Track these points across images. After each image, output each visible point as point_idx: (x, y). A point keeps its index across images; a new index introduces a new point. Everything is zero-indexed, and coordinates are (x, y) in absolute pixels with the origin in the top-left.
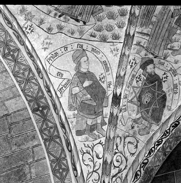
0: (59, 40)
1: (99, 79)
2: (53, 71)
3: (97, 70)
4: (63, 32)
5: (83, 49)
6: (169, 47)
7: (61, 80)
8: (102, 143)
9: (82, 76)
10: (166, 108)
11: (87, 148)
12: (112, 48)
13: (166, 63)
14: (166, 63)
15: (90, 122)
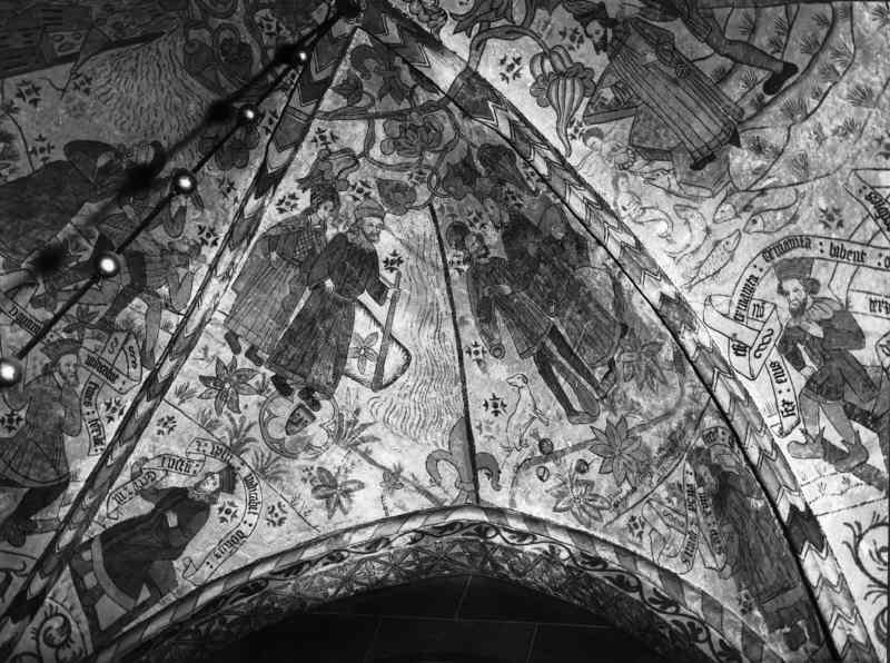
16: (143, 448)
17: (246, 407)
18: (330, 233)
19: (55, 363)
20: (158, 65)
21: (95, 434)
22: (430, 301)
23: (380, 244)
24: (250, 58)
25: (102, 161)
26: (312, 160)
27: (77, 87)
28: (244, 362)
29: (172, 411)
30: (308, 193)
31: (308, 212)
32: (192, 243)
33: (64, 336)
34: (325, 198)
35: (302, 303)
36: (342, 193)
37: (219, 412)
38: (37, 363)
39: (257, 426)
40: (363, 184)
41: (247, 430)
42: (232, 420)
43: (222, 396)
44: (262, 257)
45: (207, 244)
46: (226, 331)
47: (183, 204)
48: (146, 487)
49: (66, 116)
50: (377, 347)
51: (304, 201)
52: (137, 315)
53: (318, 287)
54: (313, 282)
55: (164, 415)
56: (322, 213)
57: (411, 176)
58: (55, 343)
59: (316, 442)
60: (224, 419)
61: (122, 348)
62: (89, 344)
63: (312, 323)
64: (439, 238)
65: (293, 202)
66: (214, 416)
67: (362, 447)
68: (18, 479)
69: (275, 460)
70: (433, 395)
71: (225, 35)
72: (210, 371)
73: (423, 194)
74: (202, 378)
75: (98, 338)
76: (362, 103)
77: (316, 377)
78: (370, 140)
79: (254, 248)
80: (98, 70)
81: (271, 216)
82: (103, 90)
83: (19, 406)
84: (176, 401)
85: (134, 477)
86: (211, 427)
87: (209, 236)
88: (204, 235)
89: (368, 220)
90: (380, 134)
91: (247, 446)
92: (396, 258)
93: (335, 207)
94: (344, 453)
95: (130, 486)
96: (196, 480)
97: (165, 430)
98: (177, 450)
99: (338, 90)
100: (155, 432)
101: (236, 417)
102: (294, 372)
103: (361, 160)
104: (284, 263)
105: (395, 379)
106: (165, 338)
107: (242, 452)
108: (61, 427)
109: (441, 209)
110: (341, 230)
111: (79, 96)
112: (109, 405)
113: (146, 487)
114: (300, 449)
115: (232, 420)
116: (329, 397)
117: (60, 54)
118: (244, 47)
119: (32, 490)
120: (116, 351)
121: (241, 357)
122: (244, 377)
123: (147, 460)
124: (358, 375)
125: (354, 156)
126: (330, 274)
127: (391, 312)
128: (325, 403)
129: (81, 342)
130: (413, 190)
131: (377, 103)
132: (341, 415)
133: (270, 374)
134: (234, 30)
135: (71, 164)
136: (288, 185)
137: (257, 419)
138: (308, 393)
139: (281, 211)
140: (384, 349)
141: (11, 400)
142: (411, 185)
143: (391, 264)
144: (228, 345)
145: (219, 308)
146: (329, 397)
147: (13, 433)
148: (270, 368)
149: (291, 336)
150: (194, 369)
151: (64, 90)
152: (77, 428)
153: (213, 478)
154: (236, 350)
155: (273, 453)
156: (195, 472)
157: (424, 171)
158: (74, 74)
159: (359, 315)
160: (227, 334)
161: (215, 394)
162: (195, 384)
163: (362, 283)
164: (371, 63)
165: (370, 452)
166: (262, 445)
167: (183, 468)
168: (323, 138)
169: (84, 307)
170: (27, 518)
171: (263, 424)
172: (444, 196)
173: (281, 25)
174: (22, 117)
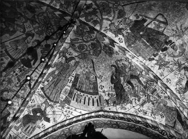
16: (173, 88)
17: (169, 60)
18: (129, 31)
19: (152, 101)
20: (98, 62)
21: (167, 98)
22: (146, 7)
23: (133, 19)
24: (94, 43)
25: (114, 78)
26: (111, 33)
27: (101, 78)
28: (157, 58)
29: (165, 79)
30: (119, 35)
31: (123, 36)
32: (129, 63)
33: (146, 97)
34: (121, 31)
35: (145, 41)
36: (120, 27)
37: (169, 67)
38: (151, 105)
39: (174, 58)
40: (118, 22)
41: (175, 61)
42: (171, 64)
43: (164, 65)
44: (132, 48)
45: (128, 60)
46: (148, 60)
47: (122, 63)
48: (183, 91)
49: (106, 82)
50: (157, 23)
51: (121, 36)
52: (143, 80)
53: (142, 36)
54: (140, 37)
55: (166, 81)
56: (124, 32)
57: (116, 10)
58: (148, 100)
59: (181, 43)
60: (171, 66)
61: (150, 85)
62: (149, 93)
63: (149, 39)
64: (130, 4)
65: (120, 39)
66: (169, 69)
67: (184, 30)
68: (174, 120)
69: (185, 55)
70: (170, 7)
71: (90, 47)
72: (158, 67)
73: (120, 8)
74: (159, 69)
75: (148, 90)
76: (98, 20)
77: (163, 40)
78: (108, 19)
79: (130, 50)
80: (98, 73)
81: (123, 45)
82: (102, 73)
83: (159, 113)
84: (163, 77)
85: (180, 93)
86: (172, 70)
87: (127, 60)
88: (127, 60)
89: (127, 22)
90: (106, 17)
91: (179, 62)
92: (136, 15)
93: (123, 29)
94: (185, 35)
95: (182, 95)
96: (185, 78)
97: (170, 81)
98: (176, 80)
99: (95, 26)
100: (169, 84)
101: (171, 63)
102: (161, 46)
103: (112, 22)
104: (135, 43)
105: (165, 18)
106: (147, 75)
107: (181, 64)
108: (165, 105)
109: (123, 3)
110: (129, 29)
111: (103, 78)
112: (162, 93)
113: (183, 91)
114: (183, 48)
115: (171, 64)
116: (168, 37)
117: (95, 79)
118: (92, 43)
119: (177, 118)
120: (150, 87)
121: (155, 58)
122: (160, 58)
123: (176, 88)
124: (163, 29)
125: (111, 24)
126: (139, 33)
127: (149, 18)
128: (170, 38)
129: (148, 94)
130: (120, 10)
131: (98, 17)
132: (174, 35)
133: (161, 52)
134: (89, 45)
135: (114, 84)
136: (116, 39)
137: (172, 58)
138: (167, 43)
139: (122, 42)
140: (158, 21)
141: (158, 114)
142: (118, 11)
143: (138, 17)
144: (152, 61)
145: (142, 61)
146: (168, 37)
147: (164, 116)
148: (159, 52)
149: (152, 45)
150: (156, 70)
151: (102, 81)
152: (166, 102)
153: (186, 73)
154: (153, 59)
155: (183, 55)
156: (183, 77)
157: (114, 7)
158: (99, 78)
159: (149, 26)
160: (149, 61)
161: (164, 67)
162: (160, 71)
163: (142, 25)
164: (89, 18)
165: (185, 27)
166: (179, 58)
167: (181, 80)
168: (106, 30)
169: (141, 91)
170: (183, 122)
171: (174, 56)
172: (119, 2)
173: (85, 36)
174: (106, 90)
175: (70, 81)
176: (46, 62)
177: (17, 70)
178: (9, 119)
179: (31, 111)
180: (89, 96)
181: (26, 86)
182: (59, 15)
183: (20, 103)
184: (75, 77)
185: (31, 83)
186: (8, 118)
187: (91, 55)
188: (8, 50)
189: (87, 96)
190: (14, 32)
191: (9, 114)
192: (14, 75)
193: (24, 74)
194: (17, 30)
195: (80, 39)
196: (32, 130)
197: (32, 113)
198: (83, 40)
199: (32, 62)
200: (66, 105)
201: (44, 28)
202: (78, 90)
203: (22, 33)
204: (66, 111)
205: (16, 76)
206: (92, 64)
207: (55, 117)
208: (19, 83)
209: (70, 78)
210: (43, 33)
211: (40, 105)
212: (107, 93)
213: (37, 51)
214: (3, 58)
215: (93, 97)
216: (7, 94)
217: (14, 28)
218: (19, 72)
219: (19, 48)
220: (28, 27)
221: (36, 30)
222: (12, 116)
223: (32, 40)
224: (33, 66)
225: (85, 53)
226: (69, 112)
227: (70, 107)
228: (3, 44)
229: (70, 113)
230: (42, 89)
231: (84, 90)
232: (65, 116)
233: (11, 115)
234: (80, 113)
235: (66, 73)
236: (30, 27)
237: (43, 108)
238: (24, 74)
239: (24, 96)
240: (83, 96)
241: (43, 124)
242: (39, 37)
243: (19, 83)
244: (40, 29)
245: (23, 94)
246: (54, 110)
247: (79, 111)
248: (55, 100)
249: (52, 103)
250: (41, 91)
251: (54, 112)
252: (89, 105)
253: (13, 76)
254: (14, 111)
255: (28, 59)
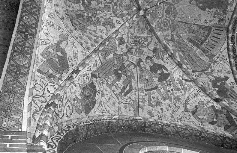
0: (58, 21)
1: (68, 58)
2: (45, 29)
3: (70, 54)
4: (63, 21)
5: (68, 38)
6: (106, 79)
7: (46, 38)
8: (55, 87)
9: (58, 48)
10: (93, 109)
11: (41, 83)
12: (83, 50)
13: (102, 86)
14: (102, 86)
15: (51, 72)
25: (201, 5)
27: (197, 19)
71: (167, 16)
175: (192, 47)
176: (169, 58)
177: (168, 88)
178: (218, 107)
179: (214, 88)
180: (210, 35)
181: (187, 85)
182: (136, 17)
183: (203, 94)
184: (189, 41)
185: (185, 79)
186: (216, 108)
187: (174, 19)
188: (146, 88)
189: (210, 37)
190: (132, 73)
191: (213, 107)
192: (172, 93)
193: (174, 83)
194: (131, 70)
195: (159, 20)
196: (234, 94)
197: (216, 89)
198: (160, 18)
199: (165, 71)
200: (215, 59)
201: (138, 46)
202: (202, 44)
203: (136, 68)
204: (221, 61)
205: (174, 91)
206: (182, 23)
207: (224, 72)
208: (182, 90)
209: (190, 46)
210: (142, 49)
211: (209, 79)
212: (212, 18)
213: (155, 63)
214: (152, 96)
215: (212, 32)
216: (190, 105)
217: (130, 71)
218: (170, 87)
219: (147, 77)
220: (132, 59)
221: (137, 55)
222: (215, 104)
223: (145, 63)
224: (169, 72)
225: (171, 24)
226: (221, 58)
227: (217, 55)
228: (139, 89)
229: (223, 57)
230: (193, 71)
231: (203, 38)
232: (225, 62)
233: (214, 105)
234: (225, 48)
235: (184, 47)
236: (133, 58)
237: (213, 79)
238: (174, 83)
239: (197, 89)
240: (209, 41)
241: (230, 84)
242: (144, 55)
243: (182, 90)
244: (138, 50)
245: (195, 89)
246: (217, 70)
247: (222, 49)
248: (207, 67)
249: (209, 69)
250: (196, 74)
251: (218, 71)
252: (219, 39)
253: (173, 94)
254: (210, 101)
255: (160, 74)
